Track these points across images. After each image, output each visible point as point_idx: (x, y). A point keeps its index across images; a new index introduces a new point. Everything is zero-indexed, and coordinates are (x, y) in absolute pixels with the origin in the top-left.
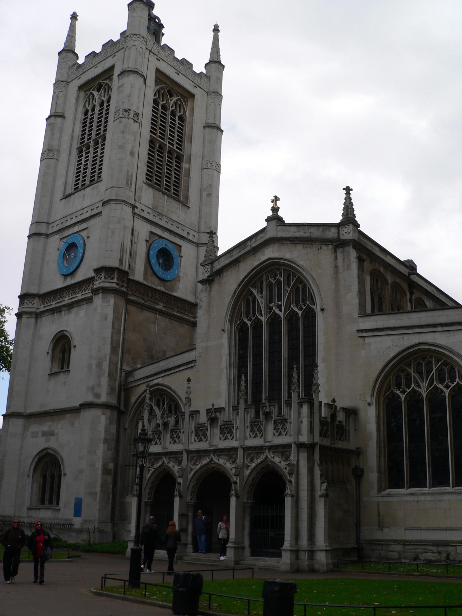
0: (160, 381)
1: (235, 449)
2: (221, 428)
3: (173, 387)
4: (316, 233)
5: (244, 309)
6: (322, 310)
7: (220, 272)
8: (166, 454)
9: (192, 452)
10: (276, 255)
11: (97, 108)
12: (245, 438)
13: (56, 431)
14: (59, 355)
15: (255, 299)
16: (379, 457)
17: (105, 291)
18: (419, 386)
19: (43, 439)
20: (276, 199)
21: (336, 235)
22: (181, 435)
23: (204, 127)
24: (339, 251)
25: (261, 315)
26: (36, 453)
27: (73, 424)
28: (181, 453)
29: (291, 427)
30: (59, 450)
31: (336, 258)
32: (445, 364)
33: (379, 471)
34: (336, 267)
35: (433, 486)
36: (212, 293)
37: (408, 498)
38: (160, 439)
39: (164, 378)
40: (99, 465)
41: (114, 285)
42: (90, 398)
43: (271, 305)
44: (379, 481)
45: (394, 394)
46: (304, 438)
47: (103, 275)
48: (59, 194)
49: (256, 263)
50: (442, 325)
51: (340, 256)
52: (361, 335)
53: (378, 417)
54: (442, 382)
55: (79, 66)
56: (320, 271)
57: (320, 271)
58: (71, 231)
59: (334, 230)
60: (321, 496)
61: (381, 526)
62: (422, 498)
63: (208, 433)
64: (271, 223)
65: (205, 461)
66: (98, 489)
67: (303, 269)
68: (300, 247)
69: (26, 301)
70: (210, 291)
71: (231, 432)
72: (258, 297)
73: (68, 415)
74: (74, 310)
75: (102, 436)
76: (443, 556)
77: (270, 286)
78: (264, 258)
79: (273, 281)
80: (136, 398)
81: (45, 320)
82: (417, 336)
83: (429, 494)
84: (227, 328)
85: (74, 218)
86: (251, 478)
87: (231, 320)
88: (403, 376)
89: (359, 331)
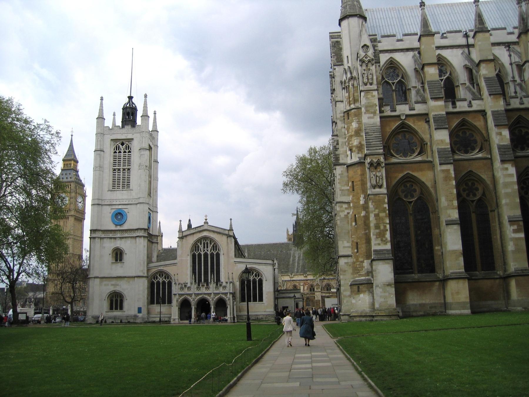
0: (162, 268)
1: (211, 294)
3: (168, 271)
6: (223, 254)
7: (186, 236)
8: (186, 294)
9: (196, 294)
11: (122, 154)
12: (214, 291)
13: (119, 284)
14: (115, 255)
17: (144, 237)
19: (113, 287)
20: (206, 216)
23: (154, 161)
24: (229, 238)
25: (201, 252)
26: (110, 291)
27: (129, 282)
28: (192, 294)
29: (228, 289)
32: (257, 273)
35: (253, 302)
38: (183, 290)
40: (146, 297)
41: (146, 235)
42: (141, 274)
44: (240, 300)
46: (231, 291)
47: (143, 231)
48: (106, 188)
49: (200, 236)
50: (257, 263)
54: (256, 277)
55: (111, 129)
58: (117, 207)
61: (240, 311)
65: (200, 296)
66: (146, 304)
68: (216, 234)
69: (97, 232)
70: (182, 241)
71: (209, 289)
72: (200, 246)
74: (123, 240)
75: (146, 287)
76: (256, 318)
78: (203, 235)
80: (151, 273)
81: (105, 240)
83: (252, 304)
84: (189, 254)
85: (118, 202)
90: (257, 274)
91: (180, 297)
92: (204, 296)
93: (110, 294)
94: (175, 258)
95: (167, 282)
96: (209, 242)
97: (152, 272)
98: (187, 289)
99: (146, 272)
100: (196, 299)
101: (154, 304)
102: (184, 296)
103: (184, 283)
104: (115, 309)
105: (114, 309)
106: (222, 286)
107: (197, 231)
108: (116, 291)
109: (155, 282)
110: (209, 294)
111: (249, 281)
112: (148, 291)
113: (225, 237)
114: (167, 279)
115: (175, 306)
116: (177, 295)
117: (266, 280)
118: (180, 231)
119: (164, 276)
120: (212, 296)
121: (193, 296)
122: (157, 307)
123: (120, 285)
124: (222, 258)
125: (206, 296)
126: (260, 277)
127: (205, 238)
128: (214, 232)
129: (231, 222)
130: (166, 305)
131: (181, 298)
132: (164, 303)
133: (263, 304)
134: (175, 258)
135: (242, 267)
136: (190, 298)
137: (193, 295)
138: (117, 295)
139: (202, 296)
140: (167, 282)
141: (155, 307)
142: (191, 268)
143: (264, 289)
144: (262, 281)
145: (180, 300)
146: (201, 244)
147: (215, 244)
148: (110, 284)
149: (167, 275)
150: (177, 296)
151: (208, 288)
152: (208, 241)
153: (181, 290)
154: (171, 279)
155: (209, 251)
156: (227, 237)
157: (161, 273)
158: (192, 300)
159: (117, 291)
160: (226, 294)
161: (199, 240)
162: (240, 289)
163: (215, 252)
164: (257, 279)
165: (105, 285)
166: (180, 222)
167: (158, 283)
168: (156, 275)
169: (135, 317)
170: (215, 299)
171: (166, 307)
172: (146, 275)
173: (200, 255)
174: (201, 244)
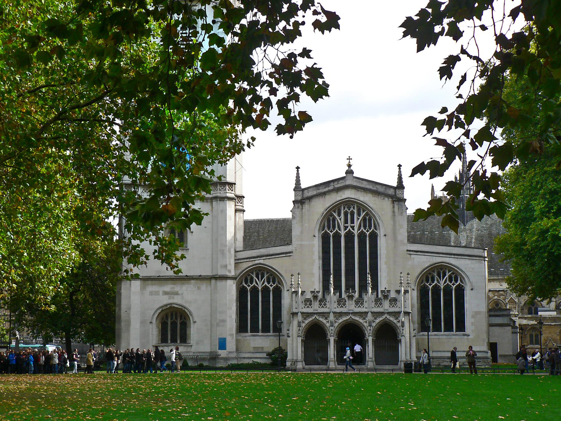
0: (262, 261)
1: (366, 313)
2: (355, 301)
4: (381, 189)
5: (326, 224)
8: (316, 313)
10: (353, 196)
13: (180, 292)
15: (334, 219)
16: (418, 316)
18: (439, 282)
20: (349, 159)
21: (394, 193)
22: (327, 303)
24: (396, 203)
25: (340, 230)
27: (199, 288)
28: (329, 313)
30: (186, 305)
31: (394, 207)
32: (453, 273)
33: (418, 324)
34: (394, 212)
35: (445, 331)
36: (303, 210)
37: (436, 337)
39: (265, 260)
43: (346, 225)
45: (425, 285)
49: (339, 199)
50: (454, 255)
51: (396, 207)
52: (409, 253)
53: (417, 296)
54: (451, 281)
56: (383, 213)
57: (383, 213)
59: (392, 190)
60: (415, 336)
62: (441, 337)
63: (347, 303)
64: (348, 175)
65: (345, 318)
66: (234, 332)
67: (372, 209)
68: (370, 195)
70: (302, 209)
71: (362, 304)
72: (338, 218)
73: (192, 281)
77: (346, 214)
79: (349, 211)
82: (440, 258)
84: (317, 235)
86: (376, 327)
87: (319, 230)
88: (430, 277)
89: (408, 250)
90: (453, 276)
91: (305, 319)
92: (353, 317)
93: (162, 311)
94: (289, 243)
95: (271, 288)
96: (355, 211)
97: (243, 269)
98: (318, 303)
99: (232, 267)
100: (336, 325)
101: (246, 331)
102: (313, 318)
103: (312, 292)
104: (172, 342)
105: (169, 341)
106: (389, 299)
107: (331, 188)
108: (173, 305)
109: (249, 288)
110: (363, 315)
111: (436, 289)
112: (237, 306)
113: (387, 204)
114: (271, 283)
115: (295, 335)
116: (299, 314)
117: (472, 289)
118: (298, 188)
119: (265, 277)
120: (370, 317)
121: (332, 317)
122: (252, 338)
123: (182, 294)
124: (382, 243)
125: (357, 318)
126: (459, 282)
127: (348, 203)
128: (365, 190)
129: (400, 172)
130: (271, 333)
131: (307, 322)
132: (266, 329)
133: (466, 337)
134: (289, 243)
135: (425, 262)
136: (324, 321)
137: (332, 314)
138: (174, 313)
139: (348, 317)
140: (271, 288)
141: (248, 338)
142: (321, 262)
143: (467, 306)
144: (463, 290)
145: (303, 325)
146: (339, 215)
147: (367, 214)
148: (161, 293)
149: (271, 275)
150: (300, 317)
151: (360, 301)
152: (354, 208)
153: (306, 305)
154: (280, 282)
155: (356, 228)
156: (393, 202)
157: (261, 271)
158: (328, 325)
159: (176, 306)
160: (396, 314)
161: (336, 207)
162: (419, 305)
163: (368, 231)
164: (454, 287)
165: (151, 293)
166: (298, 171)
167: (255, 290)
168: (249, 275)
169: (214, 357)
170: (374, 325)
171: (272, 338)
172: (233, 274)
173: (337, 236)
174: (339, 215)
